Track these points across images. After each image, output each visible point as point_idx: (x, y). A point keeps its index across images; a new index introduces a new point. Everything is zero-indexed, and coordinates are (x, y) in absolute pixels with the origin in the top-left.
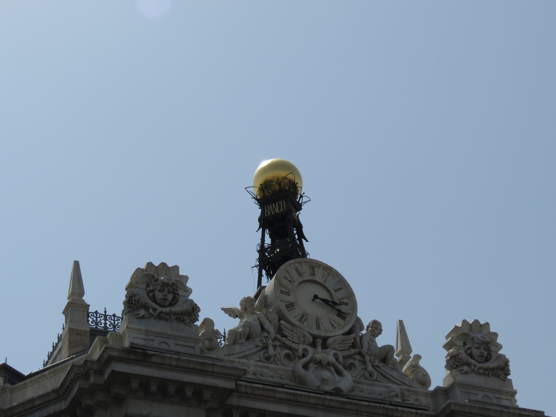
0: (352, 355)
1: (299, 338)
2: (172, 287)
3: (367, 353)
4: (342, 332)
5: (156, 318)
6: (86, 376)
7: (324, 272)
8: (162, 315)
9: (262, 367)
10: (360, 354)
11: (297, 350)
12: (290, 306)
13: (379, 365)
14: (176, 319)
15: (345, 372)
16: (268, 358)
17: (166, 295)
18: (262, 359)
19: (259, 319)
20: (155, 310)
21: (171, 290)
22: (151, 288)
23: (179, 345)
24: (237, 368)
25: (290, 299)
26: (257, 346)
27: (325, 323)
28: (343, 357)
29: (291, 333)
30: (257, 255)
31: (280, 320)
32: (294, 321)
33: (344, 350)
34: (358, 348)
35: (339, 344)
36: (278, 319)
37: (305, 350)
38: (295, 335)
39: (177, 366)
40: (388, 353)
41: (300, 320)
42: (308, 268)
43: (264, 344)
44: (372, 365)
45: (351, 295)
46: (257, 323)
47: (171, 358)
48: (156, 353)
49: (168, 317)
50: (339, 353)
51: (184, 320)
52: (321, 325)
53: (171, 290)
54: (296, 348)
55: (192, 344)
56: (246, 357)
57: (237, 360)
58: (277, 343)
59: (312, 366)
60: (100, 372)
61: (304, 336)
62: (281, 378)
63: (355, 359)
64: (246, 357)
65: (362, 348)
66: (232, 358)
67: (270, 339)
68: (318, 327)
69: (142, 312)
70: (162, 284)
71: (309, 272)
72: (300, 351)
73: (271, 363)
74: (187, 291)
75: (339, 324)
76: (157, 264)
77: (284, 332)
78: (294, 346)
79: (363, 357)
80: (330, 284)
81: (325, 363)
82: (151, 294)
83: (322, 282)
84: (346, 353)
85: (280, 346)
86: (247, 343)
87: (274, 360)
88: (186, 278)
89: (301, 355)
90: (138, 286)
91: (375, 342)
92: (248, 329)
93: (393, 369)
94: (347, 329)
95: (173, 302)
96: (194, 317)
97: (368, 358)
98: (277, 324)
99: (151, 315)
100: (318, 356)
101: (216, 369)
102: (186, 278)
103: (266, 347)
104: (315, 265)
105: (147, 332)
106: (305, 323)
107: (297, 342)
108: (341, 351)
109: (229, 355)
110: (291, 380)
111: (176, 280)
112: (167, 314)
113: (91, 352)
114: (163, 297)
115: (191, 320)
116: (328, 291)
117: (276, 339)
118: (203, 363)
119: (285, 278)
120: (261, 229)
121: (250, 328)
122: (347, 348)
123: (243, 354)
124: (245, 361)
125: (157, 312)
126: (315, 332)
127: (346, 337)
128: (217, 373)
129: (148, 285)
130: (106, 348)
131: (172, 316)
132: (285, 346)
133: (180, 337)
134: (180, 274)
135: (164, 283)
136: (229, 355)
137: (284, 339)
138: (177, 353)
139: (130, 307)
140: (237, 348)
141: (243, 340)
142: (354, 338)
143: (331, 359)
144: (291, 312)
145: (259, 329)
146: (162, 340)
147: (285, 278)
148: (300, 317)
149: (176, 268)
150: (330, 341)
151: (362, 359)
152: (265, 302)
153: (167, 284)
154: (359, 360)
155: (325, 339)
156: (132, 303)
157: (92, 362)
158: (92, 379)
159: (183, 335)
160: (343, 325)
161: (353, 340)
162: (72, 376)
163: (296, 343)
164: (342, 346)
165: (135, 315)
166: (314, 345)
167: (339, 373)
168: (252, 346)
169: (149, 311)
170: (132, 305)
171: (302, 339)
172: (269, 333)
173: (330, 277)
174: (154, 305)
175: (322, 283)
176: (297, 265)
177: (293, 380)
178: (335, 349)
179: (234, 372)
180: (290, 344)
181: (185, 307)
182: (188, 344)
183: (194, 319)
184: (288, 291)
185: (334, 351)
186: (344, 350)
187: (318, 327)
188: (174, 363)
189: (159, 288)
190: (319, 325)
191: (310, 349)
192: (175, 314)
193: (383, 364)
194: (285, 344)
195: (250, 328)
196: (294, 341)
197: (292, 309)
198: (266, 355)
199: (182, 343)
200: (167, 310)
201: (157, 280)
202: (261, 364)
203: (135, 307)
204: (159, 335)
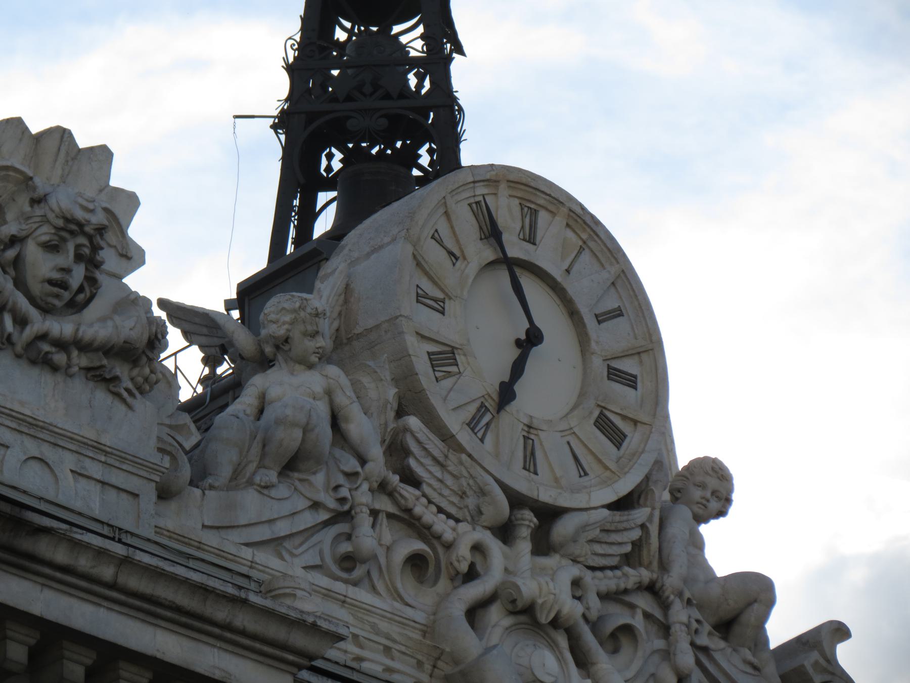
0: (626, 591)
1: (463, 495)
2: (90, 238)
3: (680, 595)
4: (612, 498)
5: (18, 356)
7: (570, 234)
8: (46, 347)
9: (328, 594)
10: (652, 589)
11: (449, 546)
12: (446, 358)
13: (712, 646)
14: (88, 369)
15: (603, 662)
16: (348, 561)
17: (67, 271)
18: (329, 561)
19: (329, 393)
20: (22, 322)
21: (87, 251)
23: (89, 478)
24: (314, 625)
25: (447, 328)
26: (316, 506)
27: (552, 447)
28: (598, 594)
30: (281, 85)
31: (400, 413)
32: (455, 423)
33: (602, 569)
34: (648, 567)
35: (591, 541)
36: (395, 406)
37: (478, 548)
38: (449, 481)
39: (113, 586)
40: (749, 604)
41: (472, 424)
42: (518, 208)
43: (342, 500)
44: (692, 644)
45: (650, 347)
46: (322, 410)
47: (101, 553)
48: (55, 524)
49: (60, 358)
50: (588, 576)
51: (116, 379)
52: (539, 454)
53: (87, 251)
54: (448, 536)
56: (275, 543)
58: (385, 504)
59: (497, 618)
61: (482, 492)
62: (387, 650)
63: (632, 607)
64: (275, 543)
65: (664, 567)
66: (230, 543)
67: (365, 486)
68: (530, 463)
70: (60, 223)
71: (518, 226)
72: (463, 554)
73: (355, 584)
74: (129, 258)
75: (600, 461)
76: (35, 127)
77: (412, 462)
78: (442, 525)
79: (665, 606)
80: (584, 287)
81: (544, 618)
83: (557, 273)
84: (609, 581)
86: (282, 491)
87: (368, 572)
88: (131, 201)
89: (464, 567)
91: (698, 543)
92: (298, 434)
93: (756, 668)
94: (624, 487)
95: (81, 297)
96: (147, 371)
97: (680, 614)
98: (392, 425)
100: (529, 588)
101: (242, 619)
102: (131, 201)
103: (344, 515)
104: (541, 202)
106: (489, 438)
107: (452, 510)
108: (593, 569)
109: (218, 528)
110: (420, 664)
111: (106, 210)
112: (61, 345)
114: (56, 276)
115: (132, 379)
116: (573, 313)
117: (383, 488)
118: (205, 591)
119: (436, 237)
122: (614, 561)
123: (264, 533)
124: (267, 559)
125: (29, 332)
126: (522, 484)
127: (618, 516)
128: (243, 633)
131: (75, 353)
132: (409, 521)
133: (98, 447)
134: (114, 182)
135: (67, 220)
136: (218, 528)
137: (408, 492)
138: (117, 534)
140: (251, 505)
141: (272, 476)
142: (643, 526)
143: (571, 608)
144: (447, 383)
145: (325, 432)
146: (33, 449)
147: (436, 237)
148: (472, 409)
149: (102, 156)
150: (563, 528)
151: (658, 613)
152: (340, 314)
153: (80, 225)
154: (647, 616)
155: (549, 515)
159: (106, 440)
160: (612, 465)
161: (636, 534)
163: (449, 516)
164: (598, 548)
166: (505, 532)
167: (583, 662)
168: (302, 504)
171: (471, 501)
172: (363, 461)
173: (586, 256)
174: (23, 302)
175: (559, 279)
176: (481, 190)
177: (428, 667)
178: (575, 561)
179: (299, 640)
180: (429, 516)
181: (127, 328)
182: (117, 478)
183: (146, 380)
184: (440, 295)
185: (575, 571)
186: (602, 569)
187: (530, 463)
188: (107, 572)
189: (45, 233)
190: (533, 454)
191: (495, 546)
192: (84, 347)
193: (722, 644)
194: (409, 511)
195: (306, 430)
196: (444, 504)
198: (345, 547)
199: (96, 470)
200: (62, 327)
201: (36, 201)
202: (324, 581)
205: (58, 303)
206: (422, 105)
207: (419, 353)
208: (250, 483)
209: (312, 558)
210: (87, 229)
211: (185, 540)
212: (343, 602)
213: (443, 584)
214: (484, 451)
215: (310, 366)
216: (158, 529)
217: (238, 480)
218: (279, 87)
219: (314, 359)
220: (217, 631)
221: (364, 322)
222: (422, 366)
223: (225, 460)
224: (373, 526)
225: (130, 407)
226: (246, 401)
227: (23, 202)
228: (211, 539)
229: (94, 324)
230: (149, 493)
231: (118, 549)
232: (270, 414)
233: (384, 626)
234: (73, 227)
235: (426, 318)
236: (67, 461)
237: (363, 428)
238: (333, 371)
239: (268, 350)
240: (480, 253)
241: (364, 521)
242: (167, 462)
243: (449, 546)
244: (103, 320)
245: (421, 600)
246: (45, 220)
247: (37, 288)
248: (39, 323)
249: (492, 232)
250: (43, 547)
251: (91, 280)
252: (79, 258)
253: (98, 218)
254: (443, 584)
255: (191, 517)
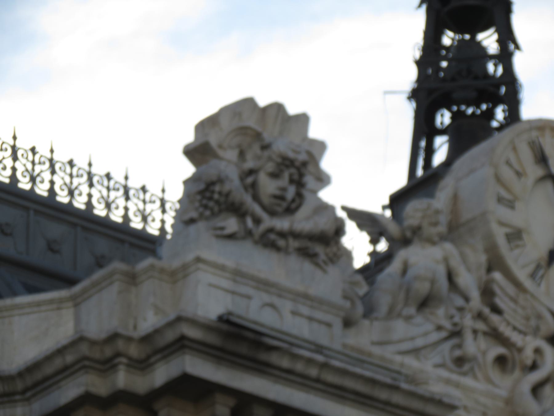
2: (298, 169)
5: (256, 243)
6: (107, 366)
8: (272, 236)
9: (448, 382)
11: (520, 350)
12: (515, 236)
16: (460, 361)
17: (284, 189)
19: (446, 260)
20: (257, 221)
21: (296, 177)
22: (250, 164)
25: (516, 218)
26: (439, 328)
29: (512, 305)
31: (489, 270)
32: (522, 275)
37: (538, 351)
38: (520, 311)
39: (317, 380)
41: (533, 276)
43: (455, 325)
47: (310, 361)
49: (281, 243)
53: (296, 177)
55: (327, 318)
56: (415, 352)
57: (398, 358)
58: (481, 326)
60: (142, 365)
61: (539, 317)
64: (415, 352)
66: (388, 352)
69: (231, 224)
72: (528, 355)
73: (465, 374)
76: (262, 102)
78: (516, 338)
82: (250, 180)
85: (485, 334)
86: (419, 319)
88: (321, 146)
89: (529, 362)
90: (221, 153)
95: (293, 206)
99: (249, 234)
102: (321, 146)
103: (456, 333)
105: (238, 275)
112: (282, 235)
113: (84, 291)
114: (278, 192)
117: (480, 316)
118: (373, 382)
119: (508, 163)
120: (424, 7)
121: (433, 282)
124: (411, 362)
125: (263, 227)
129: (242, 154)
130: (179, 319)
132: (495, 336)
133: (306, 297)
137: (495, 318)
138: (319, 349)
139: (206, 207)
140: (400, 328)
141: (412, 310)
144: (517, 252)
145: (443, 283)
147: (508, 163)
149: (303, 119)
156: (211, 199)
157: (129, 339)
158: (122, 379)
159: (312, 291)
162: (69, 358)
163: (520, 332)
165: (216, 229)
169: (244, 223)
170: (211, 204)
171: (533, 322)
172: (467, 299)
174: (258, 210)
176: (534, 134)
180: (507, 331)
182: (319, 315)
188: (313, 372)
189: (270, 167)
192: (296, 235)
197: (517, 246)
198: (458, 353)
201: (265, 147)
202: (444, 373)
203: (216, 209)
204: (264, 285)
205: (280, 209)
206: (496, 82)
207: (500, 234)
208: (399, 315)
209: (437, 360)
210: (297, 164)
211: (360, 351)
212: (457, 385)
213: (517, 373)
214: (540, 291)
215: (433, 243)
216: (345, 346)
217: (392, 313)
218: (411, 74)
219: (436, 239)
220: (381, 406)
221: (466, 215)
222: (501, 241)
223: (384, 302)
224: (475, 339)
225: (325, 271)
226: (395, 266)
227: (256, 148)
228: (377, 350)
229: (302, 221)
230: (338, 323)
231: (320, 358)
232: (411, 273)
233: (482, 399)
234: (287, 163)
235: (503, 212)
236: (287, 306)
237: (467, 280)
238: (448, 246)
239: (408, 234)
240: (535, 171)
241: (469, 337)
242: (348, 304)
243: (520, 350)
244: (308, 218)
245: (504, 384)
246: (270, 159)
247: (266, 200)
248: (268, 222)
249: (542, 159)
250: (275, 359)
251: (299, 196)
252: (292, 181)
253: (302, 157)
254: (517, 373)
255: (364, 337)
